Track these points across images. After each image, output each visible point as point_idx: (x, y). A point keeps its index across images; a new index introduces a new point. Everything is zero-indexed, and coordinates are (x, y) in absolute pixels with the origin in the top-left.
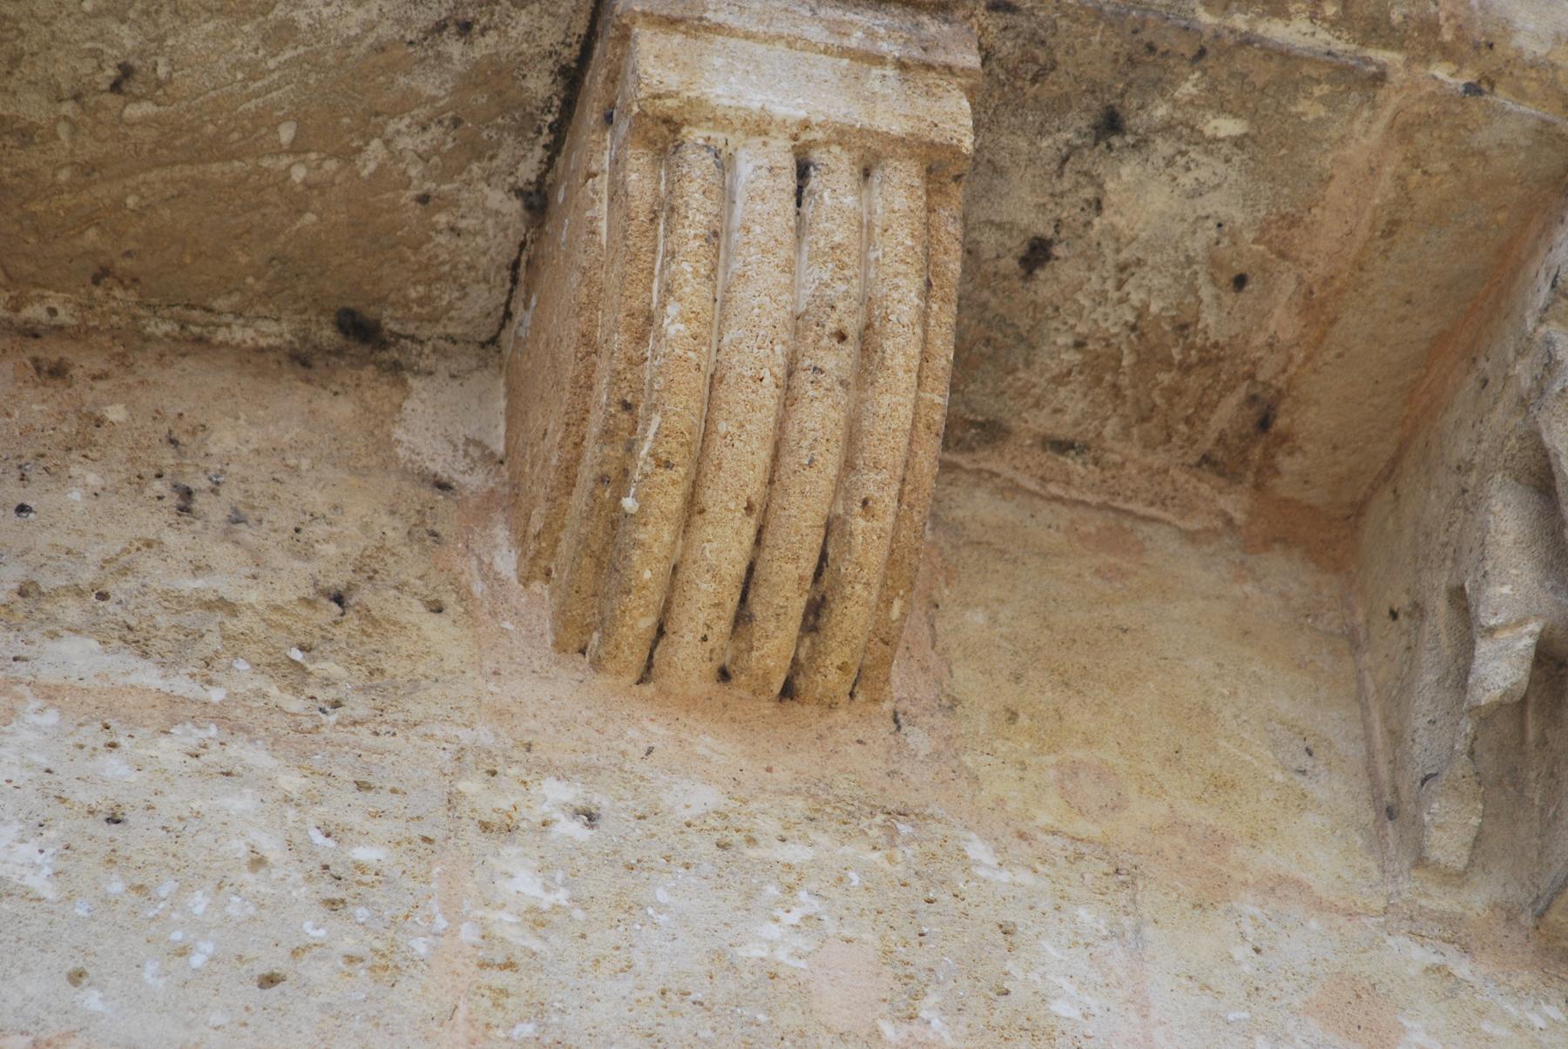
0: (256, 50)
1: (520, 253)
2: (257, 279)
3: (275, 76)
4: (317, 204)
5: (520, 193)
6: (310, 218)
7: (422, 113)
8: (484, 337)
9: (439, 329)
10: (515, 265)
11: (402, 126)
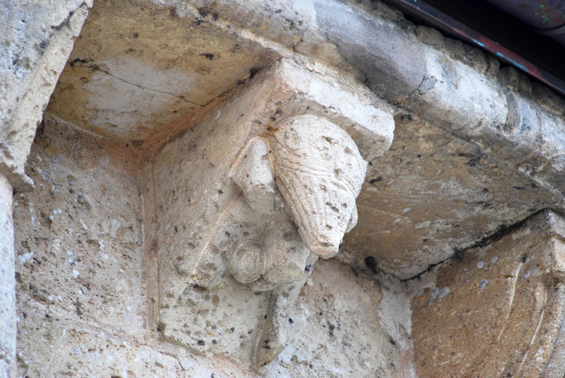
0: (421, 188)
1: (438, 264)
2: (355, 240)
3: (420, 196)
4: (394, 230)
5: (455, 249)
6: (388, 232)
7: (450, 220)
8: (403, 278)
9: (392, 272)
10: (433, 265)
11: (441, 222)
